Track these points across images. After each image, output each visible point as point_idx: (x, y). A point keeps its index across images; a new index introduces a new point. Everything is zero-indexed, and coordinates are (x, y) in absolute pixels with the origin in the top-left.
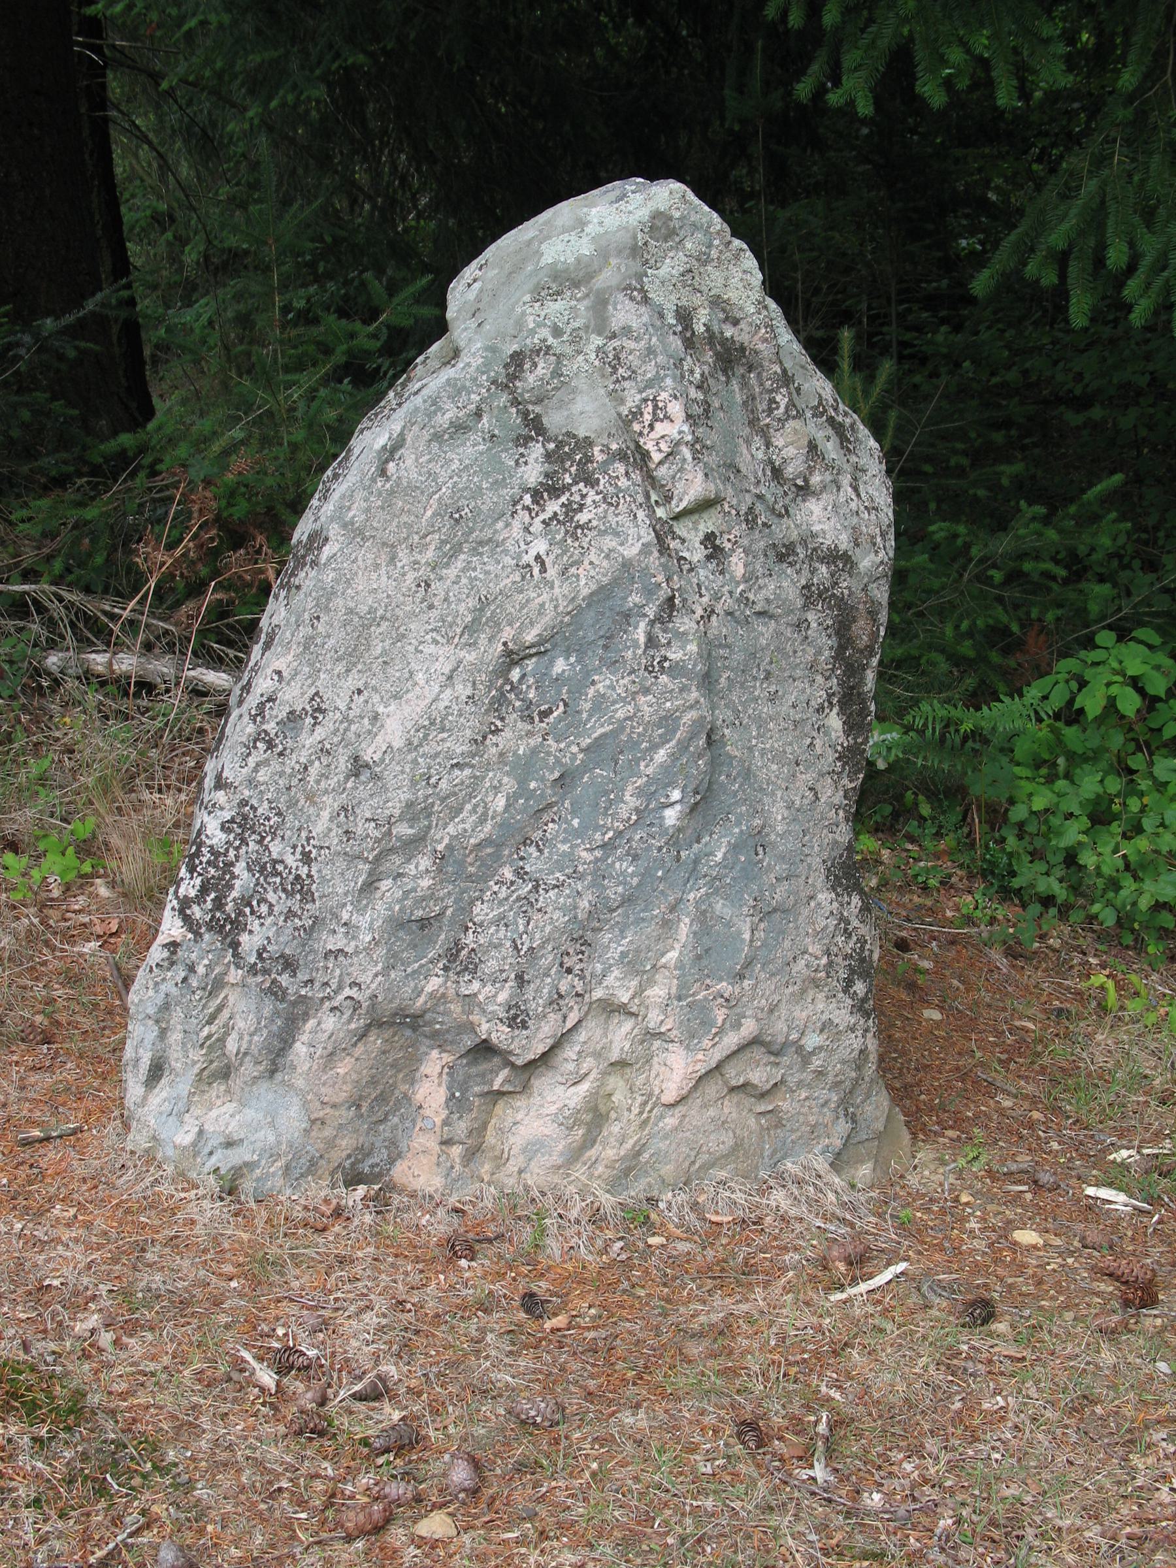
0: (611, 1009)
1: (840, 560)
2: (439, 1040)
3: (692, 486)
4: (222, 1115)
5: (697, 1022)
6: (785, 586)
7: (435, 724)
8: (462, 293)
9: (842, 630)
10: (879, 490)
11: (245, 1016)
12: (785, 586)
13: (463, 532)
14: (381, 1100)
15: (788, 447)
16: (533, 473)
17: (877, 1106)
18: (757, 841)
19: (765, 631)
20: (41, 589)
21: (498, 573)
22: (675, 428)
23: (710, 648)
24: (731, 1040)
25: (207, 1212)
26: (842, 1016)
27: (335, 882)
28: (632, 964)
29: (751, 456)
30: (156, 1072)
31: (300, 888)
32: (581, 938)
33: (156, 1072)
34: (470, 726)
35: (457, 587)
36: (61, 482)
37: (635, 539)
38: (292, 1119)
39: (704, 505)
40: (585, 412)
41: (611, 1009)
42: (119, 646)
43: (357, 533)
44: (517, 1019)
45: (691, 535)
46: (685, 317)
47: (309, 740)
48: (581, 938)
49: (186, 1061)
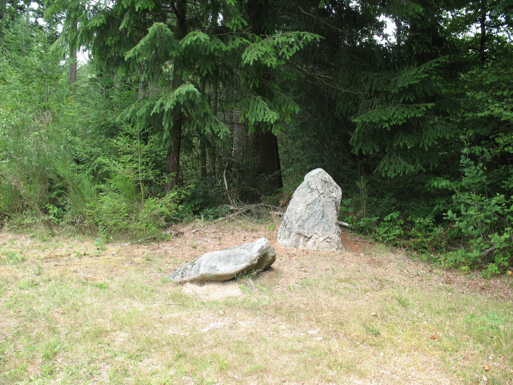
0: (316, 234)
1: (335, 198)
2: (302, 236)
3: (321, 192)
4: (285, 241)
5: (323, 235)
6: (331, 200)
7: (302, 210)
8: (306, 177)
9: (336, 203)
10: (340, 193)
11: (287, 233)
12: (331, 200)
13: (304, 195)
14: (297, 241)
15: (331, 189)
16: (309, 191)
17: (341, 246)
18: (328, 220)
19: (329, 203)
20: (269, 205)
21: (306, 198)
22: (320, 187)
23: (323, 204)
24: (326, 237)
25: (283, 247)
26: (337, 236)
27: (294, 222)
28: (317, 230)
29: (327, 190)
30: (280, 238)
31: (291, 223)
32: (313, 227)
33: (280, 238)
34: (305, 210)
35: (304, 199)
36: (271, 195)
37: (317, 196)
38: (290, 242)
39: (323, 193)
40: (313, 186)
41: (316, 234)
42: (278, 211)
43: (296, 195)
44: (308, 234)
45: (322, 196)
46: (321, 179)
47: (292, 211)
48: (313, 227)
49: (282, 237)
